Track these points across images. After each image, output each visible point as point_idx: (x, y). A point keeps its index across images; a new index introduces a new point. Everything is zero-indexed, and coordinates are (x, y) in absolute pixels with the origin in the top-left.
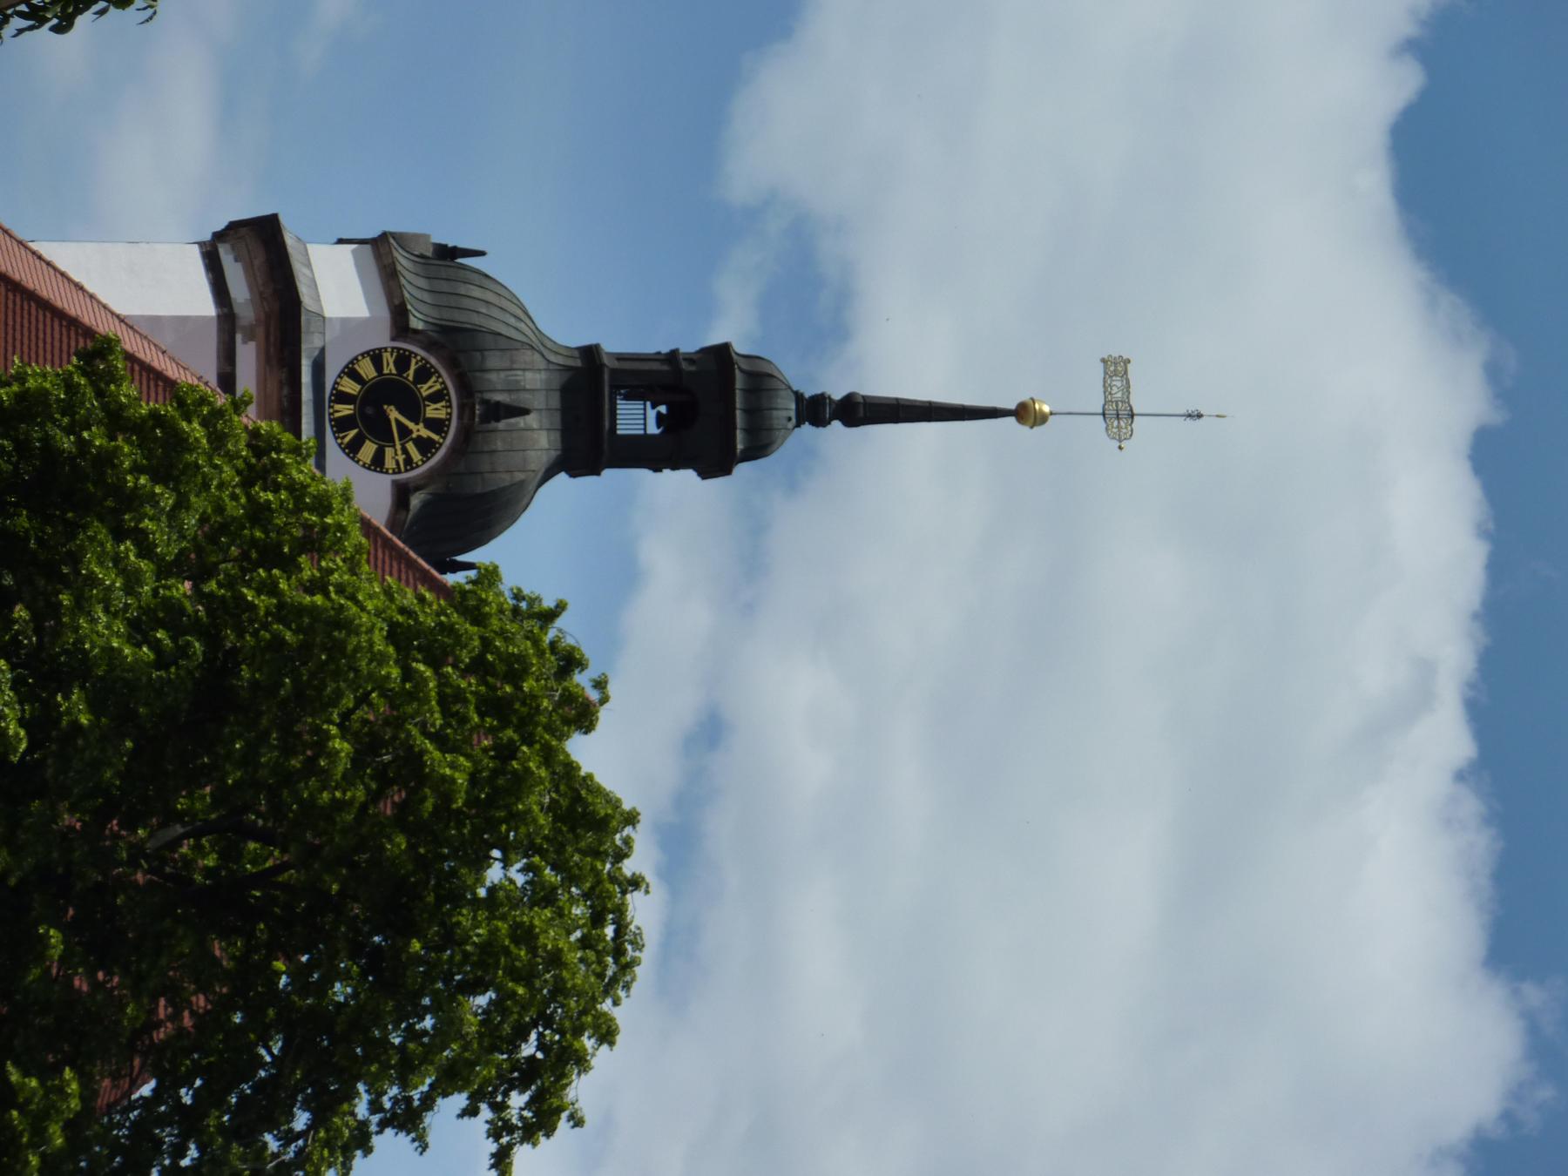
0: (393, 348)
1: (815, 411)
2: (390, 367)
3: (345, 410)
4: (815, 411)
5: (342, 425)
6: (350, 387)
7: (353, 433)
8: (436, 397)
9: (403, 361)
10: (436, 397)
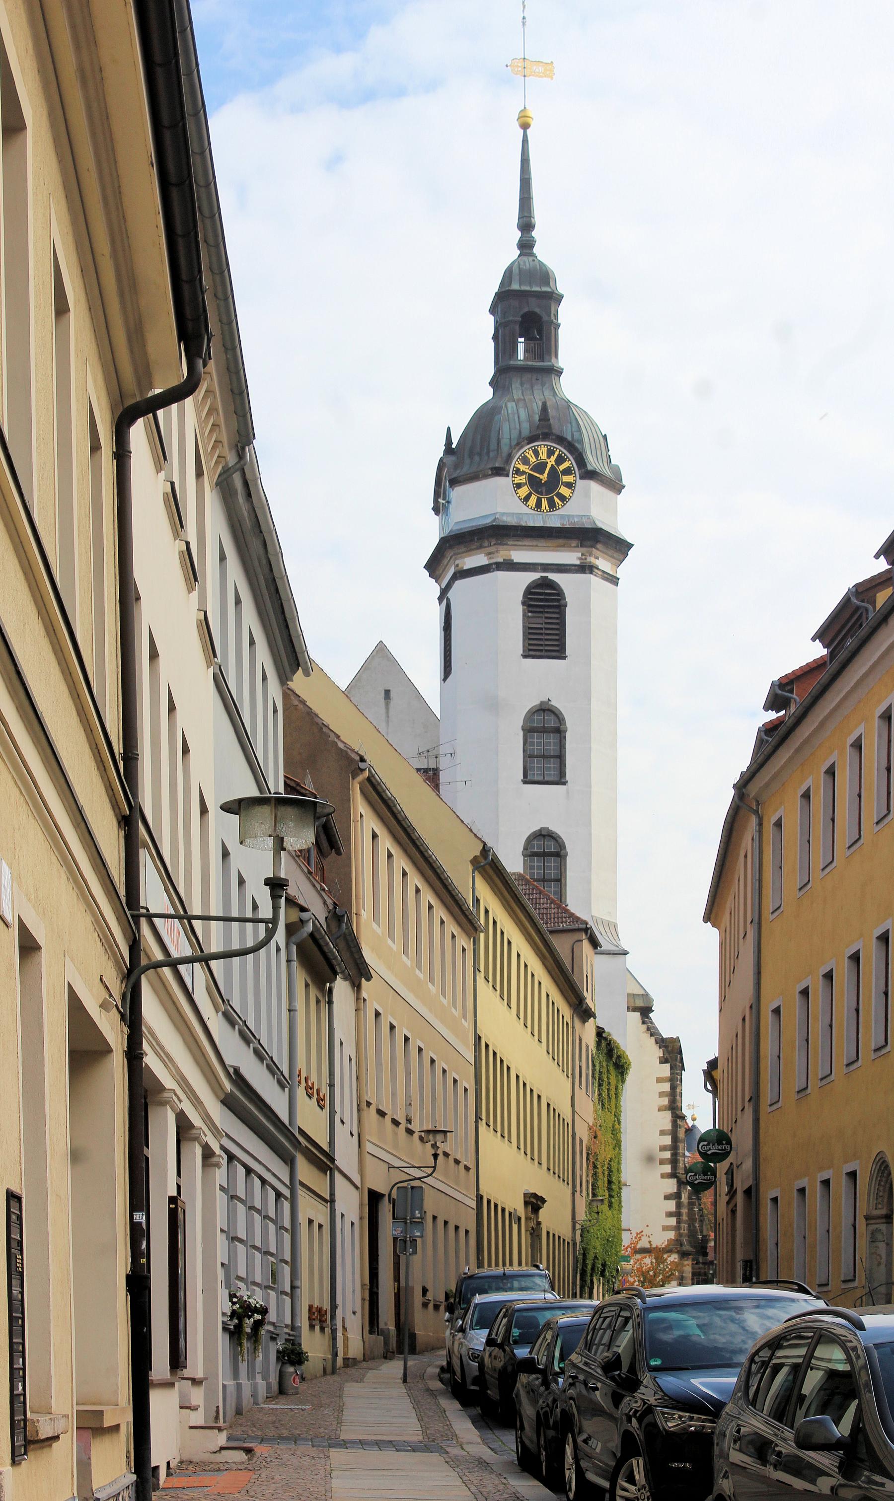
0: (513, 477)
1: (526, 246)
2: (522, 479)
3: (545, 503)
4: (526, 246)
5: (552, 504)
6: (533, 500)
7: (556, 499)
8: (536, 453)
9: (518, 472)
10: (536, 453)
